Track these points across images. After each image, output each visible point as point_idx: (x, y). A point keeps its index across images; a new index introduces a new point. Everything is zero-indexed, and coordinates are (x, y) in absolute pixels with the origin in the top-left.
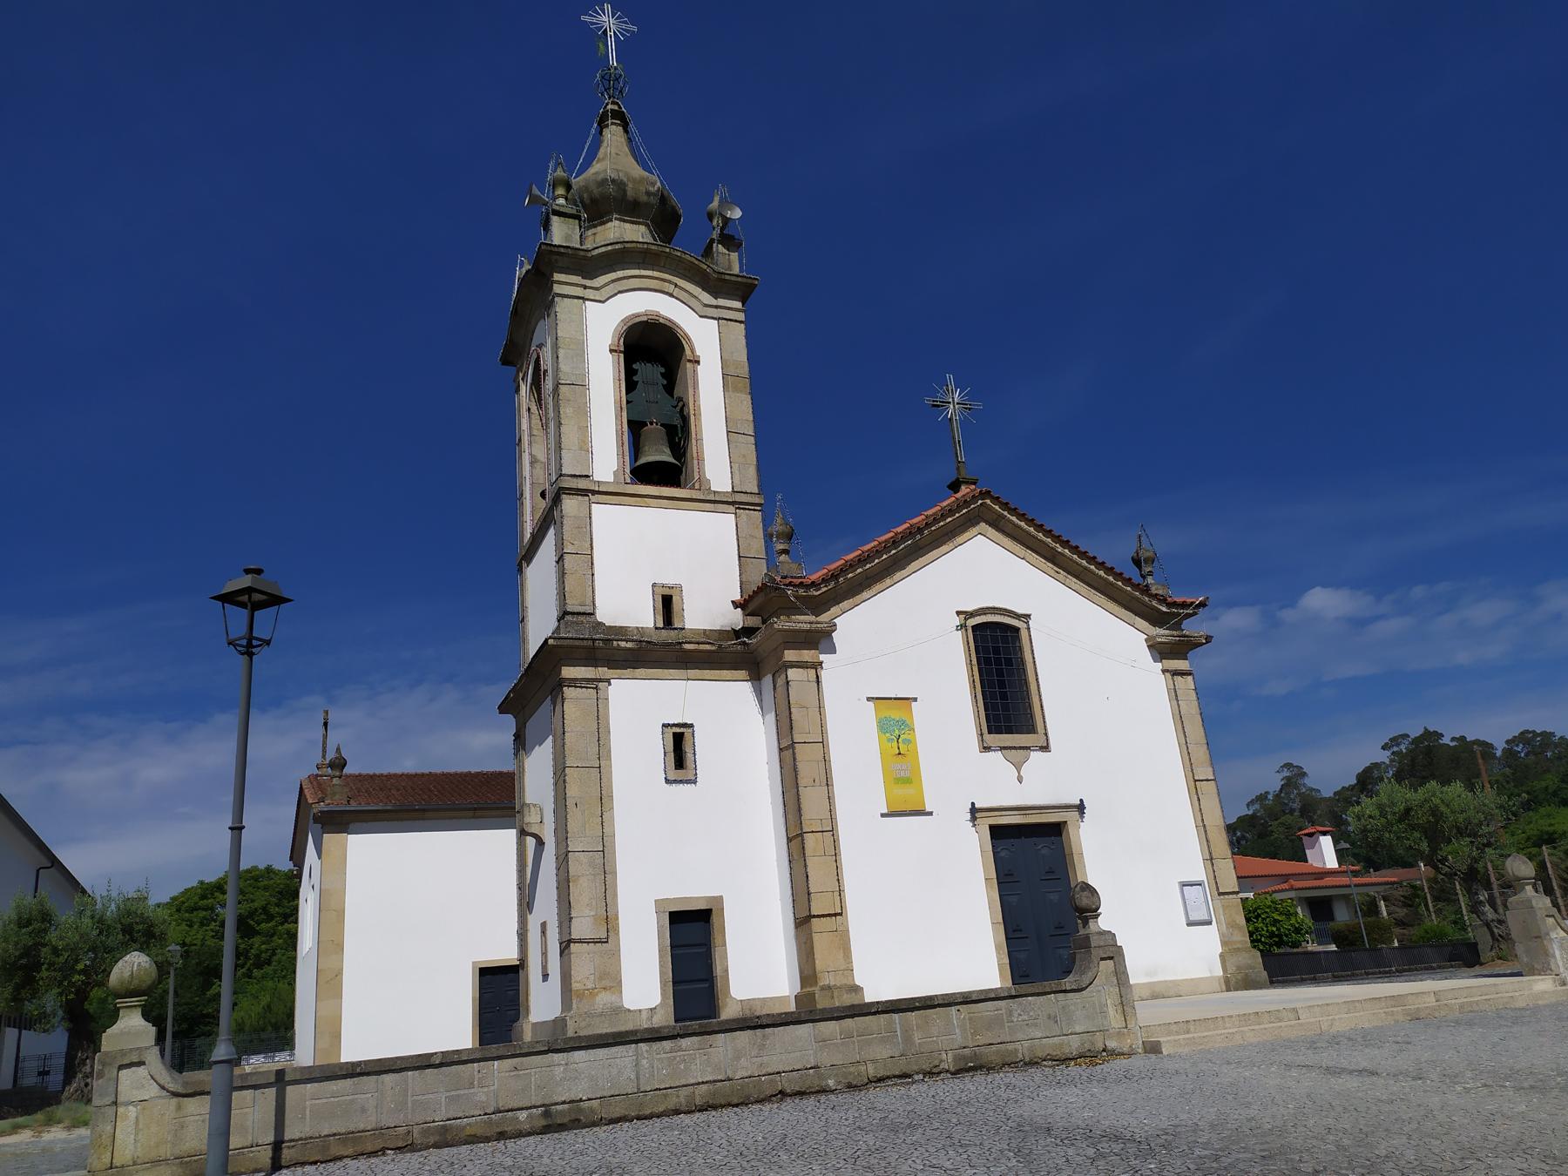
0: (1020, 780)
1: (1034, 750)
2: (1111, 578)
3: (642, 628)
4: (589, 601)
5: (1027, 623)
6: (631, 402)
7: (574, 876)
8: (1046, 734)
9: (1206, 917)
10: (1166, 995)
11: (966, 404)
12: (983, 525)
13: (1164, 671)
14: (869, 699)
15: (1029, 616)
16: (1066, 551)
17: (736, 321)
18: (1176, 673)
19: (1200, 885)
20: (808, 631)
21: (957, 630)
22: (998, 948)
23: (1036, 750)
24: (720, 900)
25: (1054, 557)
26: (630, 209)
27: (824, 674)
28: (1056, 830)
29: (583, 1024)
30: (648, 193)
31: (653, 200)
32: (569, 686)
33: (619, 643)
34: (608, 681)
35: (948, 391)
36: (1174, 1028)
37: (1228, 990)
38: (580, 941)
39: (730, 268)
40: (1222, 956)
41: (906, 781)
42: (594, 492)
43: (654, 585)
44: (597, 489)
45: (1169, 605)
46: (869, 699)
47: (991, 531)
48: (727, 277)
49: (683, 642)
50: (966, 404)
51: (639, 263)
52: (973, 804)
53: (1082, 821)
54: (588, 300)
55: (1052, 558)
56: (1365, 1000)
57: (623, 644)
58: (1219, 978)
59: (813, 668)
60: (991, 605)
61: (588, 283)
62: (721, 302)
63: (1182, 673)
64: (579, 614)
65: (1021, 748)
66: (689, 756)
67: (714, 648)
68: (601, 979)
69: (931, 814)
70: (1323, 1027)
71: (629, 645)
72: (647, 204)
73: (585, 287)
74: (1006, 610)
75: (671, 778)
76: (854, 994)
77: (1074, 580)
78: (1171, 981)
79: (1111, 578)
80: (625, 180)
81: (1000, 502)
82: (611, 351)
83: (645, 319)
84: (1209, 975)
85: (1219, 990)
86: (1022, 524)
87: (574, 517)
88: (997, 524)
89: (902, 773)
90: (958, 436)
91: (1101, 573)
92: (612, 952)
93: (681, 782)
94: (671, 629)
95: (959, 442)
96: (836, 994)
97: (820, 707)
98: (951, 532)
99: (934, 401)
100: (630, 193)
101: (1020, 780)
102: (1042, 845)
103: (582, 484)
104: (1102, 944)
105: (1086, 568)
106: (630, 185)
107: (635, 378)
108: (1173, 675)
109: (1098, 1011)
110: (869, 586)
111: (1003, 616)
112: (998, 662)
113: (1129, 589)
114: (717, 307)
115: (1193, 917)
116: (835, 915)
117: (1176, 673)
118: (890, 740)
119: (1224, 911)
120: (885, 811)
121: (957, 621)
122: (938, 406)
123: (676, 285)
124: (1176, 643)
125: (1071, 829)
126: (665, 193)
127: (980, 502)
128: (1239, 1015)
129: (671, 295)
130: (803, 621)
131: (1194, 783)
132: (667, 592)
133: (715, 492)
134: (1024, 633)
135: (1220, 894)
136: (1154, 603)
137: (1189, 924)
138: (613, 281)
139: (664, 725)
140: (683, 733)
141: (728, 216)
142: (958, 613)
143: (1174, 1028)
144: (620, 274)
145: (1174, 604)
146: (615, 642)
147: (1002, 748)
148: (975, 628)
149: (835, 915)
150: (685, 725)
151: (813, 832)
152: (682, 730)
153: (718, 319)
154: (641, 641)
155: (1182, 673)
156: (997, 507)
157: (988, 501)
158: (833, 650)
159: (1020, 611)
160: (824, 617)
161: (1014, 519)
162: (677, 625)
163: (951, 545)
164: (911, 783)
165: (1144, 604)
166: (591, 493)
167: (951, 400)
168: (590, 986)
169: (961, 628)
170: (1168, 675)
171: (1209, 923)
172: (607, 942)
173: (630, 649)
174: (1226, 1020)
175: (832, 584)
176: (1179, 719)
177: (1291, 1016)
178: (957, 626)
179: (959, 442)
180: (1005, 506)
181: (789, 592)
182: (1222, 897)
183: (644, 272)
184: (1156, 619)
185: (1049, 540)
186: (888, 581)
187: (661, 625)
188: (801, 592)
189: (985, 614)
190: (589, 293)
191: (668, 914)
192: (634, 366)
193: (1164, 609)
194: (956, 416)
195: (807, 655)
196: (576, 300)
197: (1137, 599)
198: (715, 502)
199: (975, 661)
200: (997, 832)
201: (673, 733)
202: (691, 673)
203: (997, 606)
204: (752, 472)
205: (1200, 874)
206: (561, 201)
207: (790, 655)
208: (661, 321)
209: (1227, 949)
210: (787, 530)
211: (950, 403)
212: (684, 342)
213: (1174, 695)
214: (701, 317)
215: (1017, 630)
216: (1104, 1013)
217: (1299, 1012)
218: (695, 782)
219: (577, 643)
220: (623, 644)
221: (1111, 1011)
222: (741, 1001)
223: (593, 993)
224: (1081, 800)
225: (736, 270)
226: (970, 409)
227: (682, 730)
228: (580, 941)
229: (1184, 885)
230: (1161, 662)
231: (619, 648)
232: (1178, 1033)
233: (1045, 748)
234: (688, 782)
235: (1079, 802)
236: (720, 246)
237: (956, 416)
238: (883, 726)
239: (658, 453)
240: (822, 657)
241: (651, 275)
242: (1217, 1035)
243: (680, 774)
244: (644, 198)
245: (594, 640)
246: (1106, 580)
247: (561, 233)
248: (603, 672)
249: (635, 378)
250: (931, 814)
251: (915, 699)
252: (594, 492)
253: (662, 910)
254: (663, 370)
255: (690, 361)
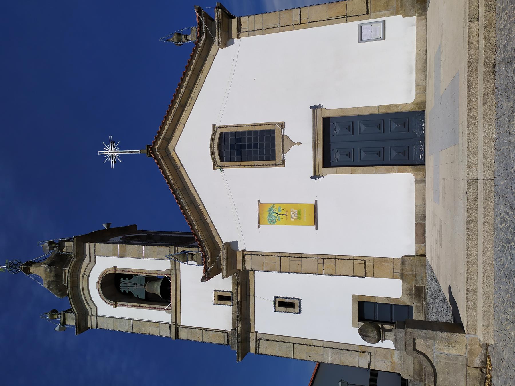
0: (299, 143)
1: (284, 133)
2: (190, 73)
3: (233, 312)
4: (223, 334)
5: (217, 128)
6: (138, 295)
7: (341, 363)
8: (275, 124)
9: (381, 24)
10: (424, 61)
11: (111, 145)
12: (169, 147)
13: (239, 38)
14: (259, 227)
15: (214, 126)
16: (177, 101)
17: (95, 247)
18: (239, 30)
19: (361, 27)
20: (227, 259)
21: (223, 171)
22: (388, 172)
23: (284, 131)
24: (354, 296)
25: (181, 106)
26: (58, 276)
27: (249, 249)
28: (326, 121)
29: (406, 372)
30: (51, 271)
31: (53, 269)
32: (259, 351)
33: (239, 330)
34: (256, 332)
35: (106, 155)
36: (471, 303)
37: (426, 15)
38: (369, 365)
39: (71, 247)
40: (404, 16)
41: (299, 212)
42: (176, 324)
43: (214, 304)
44: (175, 323)
45: (201, 35)
46: (259, 227)
47: (172, 143)
48: (75, 253)
49: (238, 302)
50: (111, 145)
51: (78, 289)
52: (312, 178)
53: (322, 106)
54: (97, 314)
55: (183, 107)
56: (469, 104)
57: (239, 329)
58: (418, 20)
59: (245, 257)
60: (209, 149)
61: (90, 314)
62: (87, 253)
63: (239, 25)
64: (228, 340)
65: (282, 142)
66: (288, 300)
67: (239, 286)
68: (387, 358)
69: (316, 201)
70: (489, 178)
71: (240, 325)
72: (55, 271)
73: (92, 315)
74: (211, 147)
75: (298, 311)
76: (406, 263)
77: (193, 93)
78: (417, 57)
79: (190, 73)
80: (47, 281)
81: (156, 141)
82: (116, 307)
83: (100, 290)
84: (415, 27)
85: (424, 21)
86: (166, 127)
87: (187, 334)
88: (168, 140)
89: (296, 215)
90: (127, 152)
91: (187, 79)
92: (375, 351)
93: (300, 307)
94: (232, 297)
95: (130, 152)
96: (405, 273)
97: (263, 254)
98: (174, 167)
99: (112, 163)
100: (52, 279)
101: (299, 143)
102: (336, 130)
103: (173, 330)
104: (403, 342)
105: (186, 88)
106: (49, 279)
107: (128, 292)
108: (241, 32)
109: (452, 362)
110: (205, 218)
111: (215, 143)
112: (238, 147)
113: (194, 61)
114: (90, 256)
115: (380, 34)
116: (365, 264)
117: (239, 30)
118: (279, 219)
119: (377, 11)
120: (314, 227)
121: (218, 170)
122: (114, 161)
123: (84, 274)
124: (223, 31)
125: (327, 115)
126: (49, 261)
127: (157, 152)
128: (468, 240)
129: (88, 276)
130: (222, 254)
131: (302, 24)
132: (216, 298)
133: (171, 269)
134: (224, 130)
135: (367, 13)
136: (201, 44)
137: (384, 39)
138: (87, 303)
139: (275, 311)
140: (278, 301)
141: (49, 248)
142: (214, 169)
143: (471, 303)
144: (83, 298)
145: (200, 31)
146: (239, 332)
147: (283, 152)
148: (222, 161)
149: (365, 264)
150: (275, 301)
151: (324, 270)
152: (277, 302)
153: (95, 256)
154: (238, 320)
155: (239, 25)
156: (159, 142)
157: (156, 147)
158: (236, 243)
159: (211, 132)
160: (221, 245)
161: (164, 132)
162: (230, 295)
163: (181, 168)
164: (300, 210)
165: (202, 51)
166: (176, 325)
167: (110, 154)
168: (389, 364)
169: (222, 168)
170: (241, 35)
171: (384, 22)
172: (371, 353)
173: (242, 325)
174: (470, 253)
175: (204, 244)
176: (266, 30)
177: (473, 186)
178: (221, 171)
179: (130, 152)
180: (157, 138)
181: (210, 268)
182: (369, 11)
183: (81, 287)
184: (209, 43)
185: (173, 111)
186: (201, 207)
187: (230, 303)
188: (209, 261)
189: (214, 153)
190: (94, 313)
191: (359, 323)
192: (122, 291)
193: (204, 38)
194: (118, 152)
195: (239, 258)
196: (98, 320)
197: (200, 55)
198: (175, 269)
199: (238, 163)
200: (327, 163)
201: (278, 307)
202: (251, 294)
203: (209, 146)
204: (161, 249)
205: (353, 26)
206: (59, 316)
207: (239, 267)
208: (100, 282)
209: (401, 12)
210: (182, 257)
211: (112, 155)
212: (108, 273)
213: (252, 32)
214: (95, 263)
215: (221, 134)
216: (453, 358)
217: (471, 178)
218: (300, 300)
219: (240, 349)
220: (239, 329)
221: (453, 352)
222: (402, 294)
223: (393, 363)
224: (311, 108)
225: (72, 243)
226: (113, 143)
227: (277, 302)
228: (369, 365)
229: (361, 40)
230: (234, 39)
231: (241, 331)
232: (475, 301)
233: (282, 125)
234: (300, 303)
235: (312, 109)
236: (64, 250)
237: (118, 152)
238: (272, 222)
239: (156, 289)
240: (240, 249)
241: (81, 284)
242: (484, 288)
243: (296, 306)
244: (53, 273)
245: (238, 342)
246: (191, 76)
247: (71, 321)
248: (252, 336)
249: (128, 292)
250: (316, 201)
251: (259, 201)
252: (176, 324)
253: (357, 325)
254: (122, 279)
255: (115, 272)
